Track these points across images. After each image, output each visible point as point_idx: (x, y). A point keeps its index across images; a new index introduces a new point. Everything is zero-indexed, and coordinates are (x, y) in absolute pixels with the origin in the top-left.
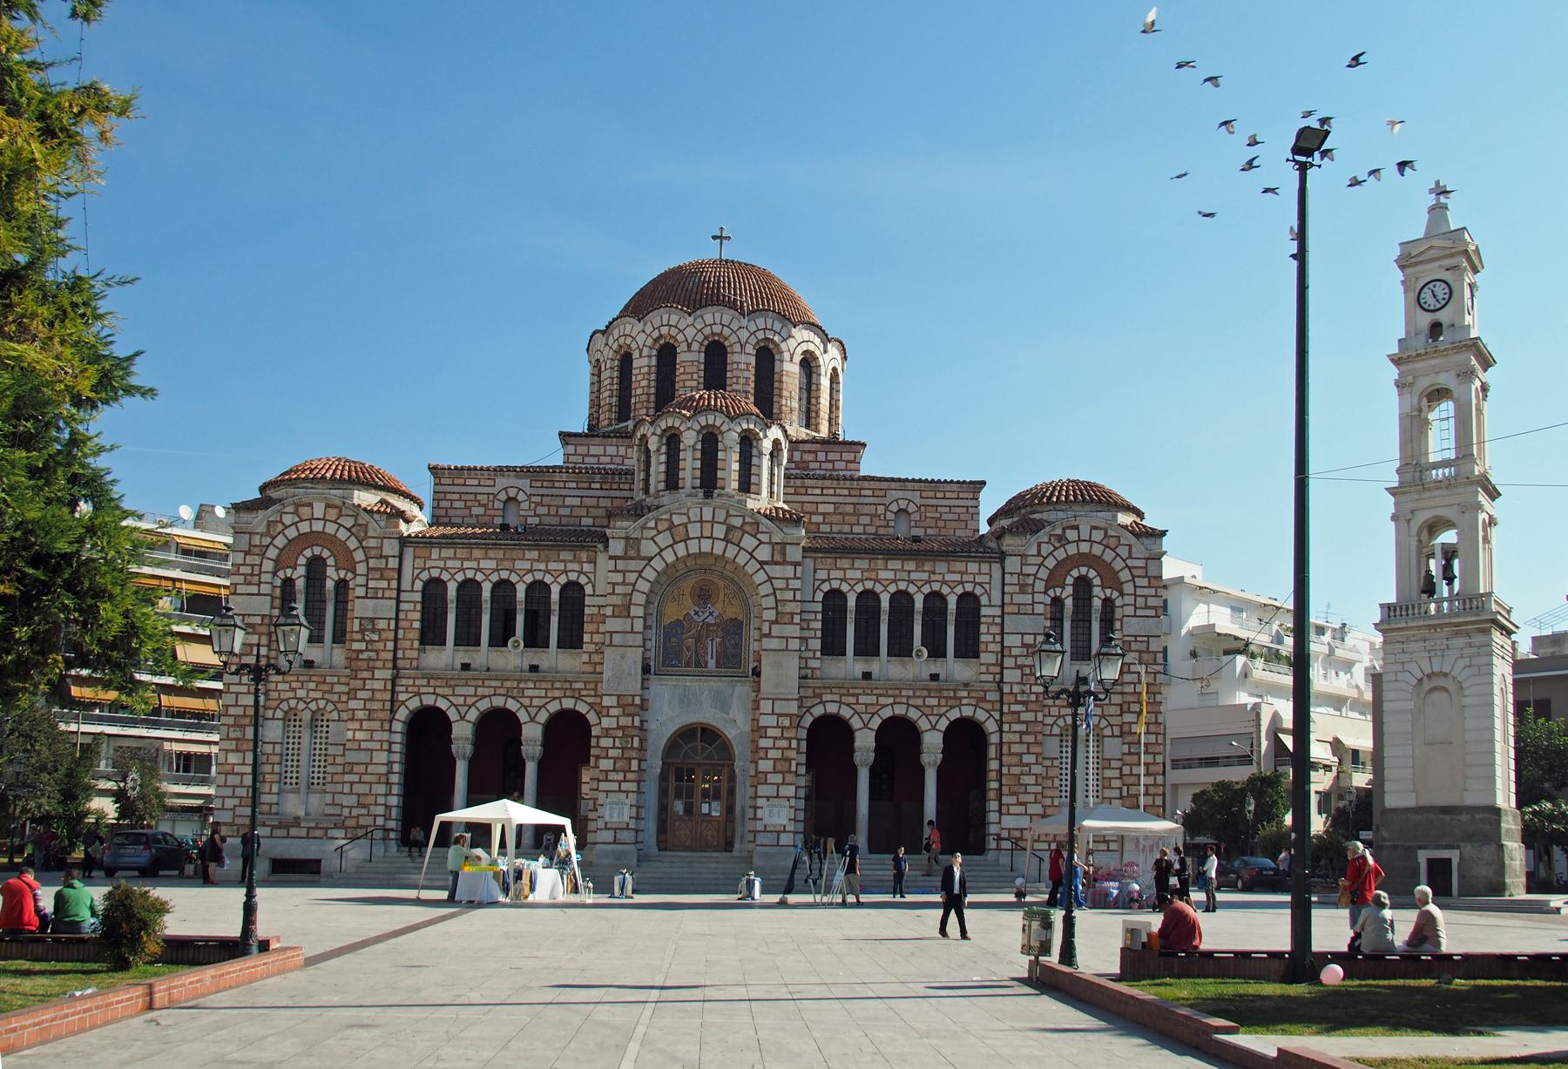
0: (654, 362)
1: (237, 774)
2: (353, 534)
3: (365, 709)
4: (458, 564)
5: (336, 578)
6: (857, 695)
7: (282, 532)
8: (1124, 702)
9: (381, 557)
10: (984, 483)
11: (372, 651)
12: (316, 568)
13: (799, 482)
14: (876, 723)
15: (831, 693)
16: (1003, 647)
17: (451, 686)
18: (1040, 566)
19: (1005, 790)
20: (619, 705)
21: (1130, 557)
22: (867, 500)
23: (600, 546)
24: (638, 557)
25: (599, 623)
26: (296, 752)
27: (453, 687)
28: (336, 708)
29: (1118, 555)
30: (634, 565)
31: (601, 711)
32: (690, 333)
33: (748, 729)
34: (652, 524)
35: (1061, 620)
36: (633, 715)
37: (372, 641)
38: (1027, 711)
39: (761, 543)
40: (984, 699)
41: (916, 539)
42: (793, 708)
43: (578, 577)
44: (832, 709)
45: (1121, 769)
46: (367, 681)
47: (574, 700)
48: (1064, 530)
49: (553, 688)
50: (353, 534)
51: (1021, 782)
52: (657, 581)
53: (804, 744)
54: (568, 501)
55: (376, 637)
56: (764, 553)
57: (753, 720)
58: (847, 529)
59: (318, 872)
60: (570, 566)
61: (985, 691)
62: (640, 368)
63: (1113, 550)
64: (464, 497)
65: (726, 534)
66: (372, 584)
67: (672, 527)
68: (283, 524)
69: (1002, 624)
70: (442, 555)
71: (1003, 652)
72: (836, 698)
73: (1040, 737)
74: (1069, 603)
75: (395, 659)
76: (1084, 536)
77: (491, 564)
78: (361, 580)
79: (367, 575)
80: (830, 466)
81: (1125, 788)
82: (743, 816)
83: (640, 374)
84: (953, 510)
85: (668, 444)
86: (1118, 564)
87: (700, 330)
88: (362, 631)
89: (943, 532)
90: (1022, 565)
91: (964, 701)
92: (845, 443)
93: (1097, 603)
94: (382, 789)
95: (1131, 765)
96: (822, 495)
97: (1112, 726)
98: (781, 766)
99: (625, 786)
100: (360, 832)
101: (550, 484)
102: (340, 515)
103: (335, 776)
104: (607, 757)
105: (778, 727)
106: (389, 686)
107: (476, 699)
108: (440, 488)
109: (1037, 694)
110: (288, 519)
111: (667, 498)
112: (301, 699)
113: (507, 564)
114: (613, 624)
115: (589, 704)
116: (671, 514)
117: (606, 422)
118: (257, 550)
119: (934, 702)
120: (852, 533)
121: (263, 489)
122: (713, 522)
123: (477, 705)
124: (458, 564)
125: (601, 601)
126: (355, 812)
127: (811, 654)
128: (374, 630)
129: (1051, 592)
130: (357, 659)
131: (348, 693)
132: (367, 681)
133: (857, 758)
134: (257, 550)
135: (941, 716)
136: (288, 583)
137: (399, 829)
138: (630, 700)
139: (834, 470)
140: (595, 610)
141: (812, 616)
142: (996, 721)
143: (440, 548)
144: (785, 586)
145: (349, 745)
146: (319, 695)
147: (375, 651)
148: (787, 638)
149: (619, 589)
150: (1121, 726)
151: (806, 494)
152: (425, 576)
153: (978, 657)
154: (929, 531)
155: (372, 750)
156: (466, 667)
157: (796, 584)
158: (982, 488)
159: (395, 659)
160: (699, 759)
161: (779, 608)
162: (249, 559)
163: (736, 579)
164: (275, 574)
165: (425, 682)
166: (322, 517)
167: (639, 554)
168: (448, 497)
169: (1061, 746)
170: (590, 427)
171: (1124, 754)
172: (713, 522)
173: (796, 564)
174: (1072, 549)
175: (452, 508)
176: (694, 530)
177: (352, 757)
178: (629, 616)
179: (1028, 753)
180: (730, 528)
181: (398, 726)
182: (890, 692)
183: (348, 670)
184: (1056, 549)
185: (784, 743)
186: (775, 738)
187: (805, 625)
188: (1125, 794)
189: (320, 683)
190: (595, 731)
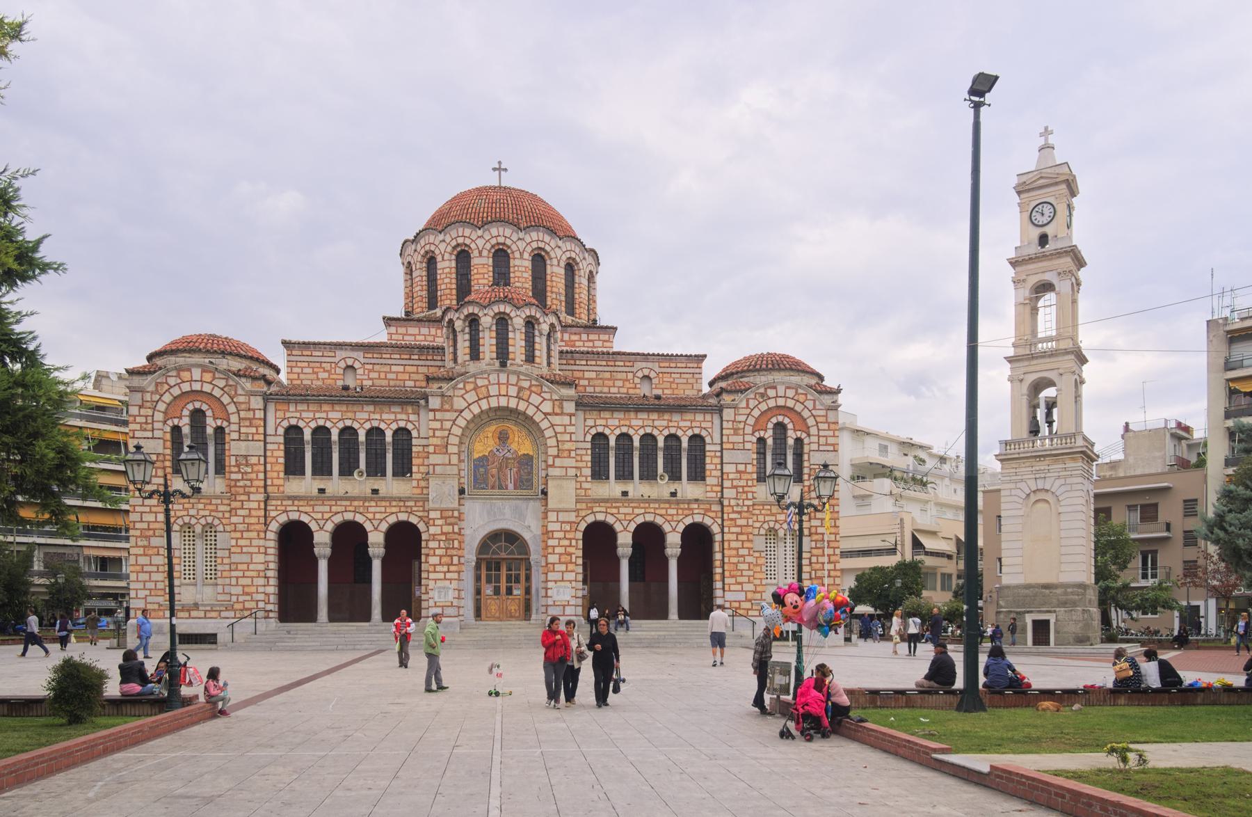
0: (454, 264)
1: (146, 572)
3: (244, 523)
4: (311, 415)
5: (215, 426)
6: (618, 508)
10: (705, 356)
11: (247, 480)
12: (197, 416)
14: (632, 527)
15: (599, 506)
16: (722, 473)
17: (310, 506)
19: (727, 573)
21: (814, 408)
22: (620, 369)
23: (422, 402)
24: (452, 410)
25: (424, 458)
26: (191, 555)
30: (448, 415)
33: (539, 533)
35: (765, 454)
36: (453, 524)
37: (246, 473)
38: (741, 518)
39: (545, 399)
41: (658, 397)
42: (572, 517)
43: (406, 424)
44: (600, 517)
45: (810, 559)
46: (245, 503)
47: (407, 514)
48: (766, 389)
52: (467, 427)
53: (580, 543)
55: (249, 470)
57: (543, 526)
58: (606, 390)
59: (215, 643)
60: (399, 416)
62: (443, 269)
63: (803, 404)
64: (311, 365)
65: (518, 393)
68: (168, 384)
69: (722, 457)
73: (751, 537)
74: (770, 442)
75: (265, 486)
76: (781, 393)
77: (338, 415)
80: (591, 344)
81: (813, 572)
83: (443, 273)
84: (683, 376)
85: (470, 326)
86: (806, 414)
88: (238, 466)
89: (676, 392)
90: (735, 415)
91: (696, 511)
92: (602, 328)
93: (791, 442)
94: (261, 581)
96: (587, 365)
98: (565, 558)
99: (449, 576)
100: (247, 613)
101: (379, 356)
102: (214, 378)
103: (224, 573)
104: (434, 555)
105: (561, 531)
106: (262, 505)
108: (292, 358)
109: (748, 506)
111: (473, 367)
112: (193, 516)
113: (350, 415)
114: (434, 459)
117: (419, 310)
118: (148, 404)
119: (674, 512)
120: (610, 393)
121: (150, 358)
122: (508, 384)
123: (333, 518)
124: (311, 415)
125: (424, 442)
126: (241, 598)
127: (584, 479)
128: (247, 465)
130: (236, 486)
131: (230, 512)
132: (245, 503)
134: (148, 404)
136: (176, 430)
137: (277, 610)
138: (450, 513)
139: (594, 347)
140: (421, 449)
141: (584, 452)
143: (296, 403)
145: (233, 550)
147: (250, 480)
148: (566, 468)
149: (438, 433)
150: (810, 529)
152: (285, 424)
153: (704, 480)
154: (666, 391)
155: (252, 553)
156: (322, 491)
158: (703, 360)
159: (265, 486)
160: (503, 555)
162: (143, 412)
163: (527, 425)
164: (165, 422)
165: (290, 502)
166: (199, 379)
167: (452, 408)
168: (299, 364)
170: (407, 313)
172: (508, 384)
173: (571, 415)
174: (772, 403)
176: (493, 390)
177: (235, 558)
178: (446, 453)
179: (743, 548)
180: (521, 389)
181: (271, 535)
182: (642, 505)
183: (229, 494)
184: (760, 403)
185: (566, 543)
186: (560, 539)
187: (579, 458)
188: (813, 576)
189: (207, 504)
190: (424, 537)
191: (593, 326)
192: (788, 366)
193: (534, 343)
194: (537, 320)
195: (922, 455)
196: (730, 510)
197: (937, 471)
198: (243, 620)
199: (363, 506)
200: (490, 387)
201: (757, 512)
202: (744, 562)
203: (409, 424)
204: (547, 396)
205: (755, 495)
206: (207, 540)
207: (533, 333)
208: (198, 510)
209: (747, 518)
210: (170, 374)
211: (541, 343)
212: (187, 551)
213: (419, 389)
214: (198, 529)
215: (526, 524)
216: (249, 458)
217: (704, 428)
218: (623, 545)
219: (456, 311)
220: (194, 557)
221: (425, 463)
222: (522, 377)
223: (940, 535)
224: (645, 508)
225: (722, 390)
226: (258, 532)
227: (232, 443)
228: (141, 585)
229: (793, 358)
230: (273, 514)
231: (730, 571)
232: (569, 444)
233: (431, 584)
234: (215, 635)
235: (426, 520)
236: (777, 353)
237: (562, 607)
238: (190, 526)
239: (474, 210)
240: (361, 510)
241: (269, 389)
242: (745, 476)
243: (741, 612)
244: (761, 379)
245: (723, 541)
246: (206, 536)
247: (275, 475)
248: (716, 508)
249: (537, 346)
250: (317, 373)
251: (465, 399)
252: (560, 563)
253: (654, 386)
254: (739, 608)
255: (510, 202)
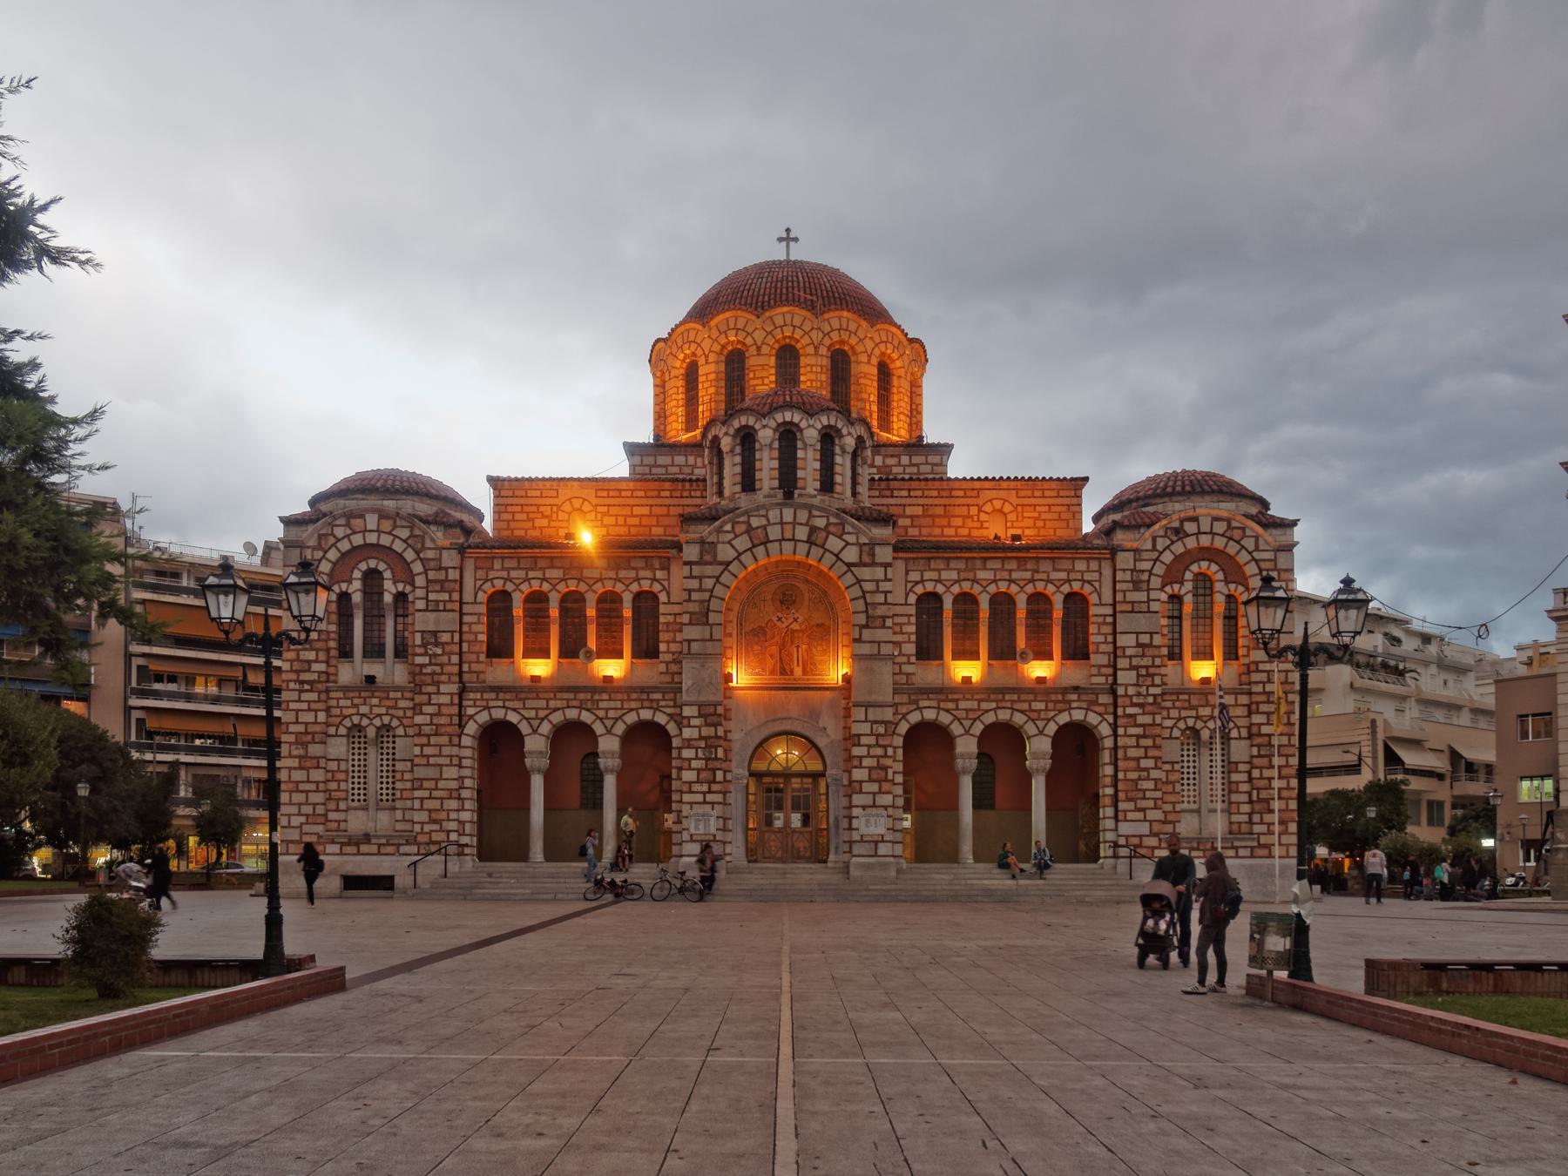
1: (302, 792)
2: (409, 545)
3: (431, 724)
5: (394, 591)
6: (956, 701)
7: (334, 545)
8: (1251, 703)
9: (441, 568)
10: (1086, 479)
13: (883, 485)
14: (978, 728)
15: (929, 699)
16: (1115, 648)
17: (520, 700)
18: (1156, 561)
19: (1121, 795)
20: (700, 715)
21: (1257, 549)
22: (958, 501)
24: (715, 562)
27: (524, 700)
28: (402, 724)
29: (1243, 547)
30: (710, 570)
31: (681, 722)
32: (759, 335)
33: (839, 736)
34: (728, 527)
36: (715, 725)
37: (435, 655)
38: (1144, 714)
39: (848, 543)
40: (1096, 703)
41: (1016, 538)
42: (888, 714)
44: (930, 715)
45: (1249, 773)
46: (433, 696)
47: (651, 711)
48: (1182, 522)
49: (629, 700)
50: (409, 545)
51: (1139, 787)
53: (900, 752)
54: (637, 510)
55: (439, 651)
56: (851, 555)
57: (845, 728)
59: (392, 888)
60: (642, 574)
61: (1097, 694)
64: (525, 509)
65: (810, 535)
66: (432, 596)
67: (750, 530)
68: (335, 536)
70: (505, 566)
71: (1116, 653)
72: (934, 704)
73: (1158, 741)
75: (461, 673)
76: (1205, 527)
78: (420, 593)
79: (427, 588)
80: (914, 470)
81: (1255, 792)
82: (837, 826)
84: (1053, 509)
85: (743, 444)
86: (1243, 557)
87: (770, 333)
88: (424, 645)
90: (1135, 560)
91: (1074, 705)
92: (929, 446)
95: (1261, 768)
97: (1238, 728)
99: (710, 798)
100: (434, 848)
102: (395, 527)
103: (404, 792)
104: (690, 768)
105: (872, 734)
106: (456, 700)
107: (548, 712)
109: (1155, 696)
110: (340, 532)
112: (364, 715)
115: (669, 715)
116: (749, 516)
119: (1041, 706)
122: (795, 523)
123: (550, 717)
124: (522, 574)
125: (677, 609)
126: (427, 828)
127: (904, 659)
128: (437, 644)
129: (1168, 589)
130: (421, 673)
131: (413, 708)
132: (433, 696)
133: (959, 763)
135: (1049, 720)
138: (712, 710)
139: (919, 473)
140: (670, 619)
141: (905, 620)
142: (1110, 724)
144: (875, 588)
145: (417, 761)
146: (383, 711)
148: (879, 643)
149: (695, 596)
150: (1249, 728)
151: (892, 497)
153: (1088, 658)
157: (885, 586)
159: (461, 673)
161: (870, 612)
165: (493, 695)
166: (375, 528)
167: (715, 560)
168: (509, 509)
169: (1182, 750)
171: (1252, 757)
172: (795, 523)
173: (886, 565)
174: (1191, 543)
175: (514, 520)
177: (421, 772)
180: (813, 530)
182: (992, 697)
184: (1173, 543)
185: (879, 751)
186: (869, 746)
187: (897, 629)
188: (1255, 798)
189: (383, 698)
190: (676, 742)
191: (916, 445)
192: (1215, 487)
193: (833, 464)
194: (839, 431)
195: (1397, 632)
196: (1127, 701)
197: (1418, 655)
198: (430, 857)
199: (592, 700)
200: (769, 529)
201: (1169, 704)
202: (1148, 779)
203: (656, 584)
204: (851, 539)
205: (1165, 679)
206: (382, 748)
207: (833, 451)
208: (372, 706)
209: (1154, 714)
210: (338, 522)
211: (842, 463)
212: (356, 763)
213: (670, 538)
214: (371, 732)
215: (821, 725)
216: (439, 634)
217: (1089, 582)
218: (963, 756)
219: (724, 423)
220: (365, 771)
221: (678, 639)
222: (815, 513)
223: (1427, 745)
224: (997, 701)
225: (1116, 525)
226: (450, 736)
227: (418, 615)
228: (294, 810)
229: (1222, 476)
230: (470, 711)
231: (1126, 792)
232: (884, 608)
233: (686, 809)
234: (391, 878)
235: (677, 718)
236: (1198, 470)
237: (873, 845)
238: (359, 728)
239: (751, 293)
240: (589, 705)
241: (467, 541)
242: (1150, 652)
243: (1143, 851)
244: (1177, 508)
245: (1116, 748)
246: (382, 742)
247: (473, 657)
248: (1105, 699)
249: (838, 469)
250: (533, 520)
251: (733, 547)
252: (871, 780)
253: (1009, 524)
254: (1140, 846)
255: (801, 279)
